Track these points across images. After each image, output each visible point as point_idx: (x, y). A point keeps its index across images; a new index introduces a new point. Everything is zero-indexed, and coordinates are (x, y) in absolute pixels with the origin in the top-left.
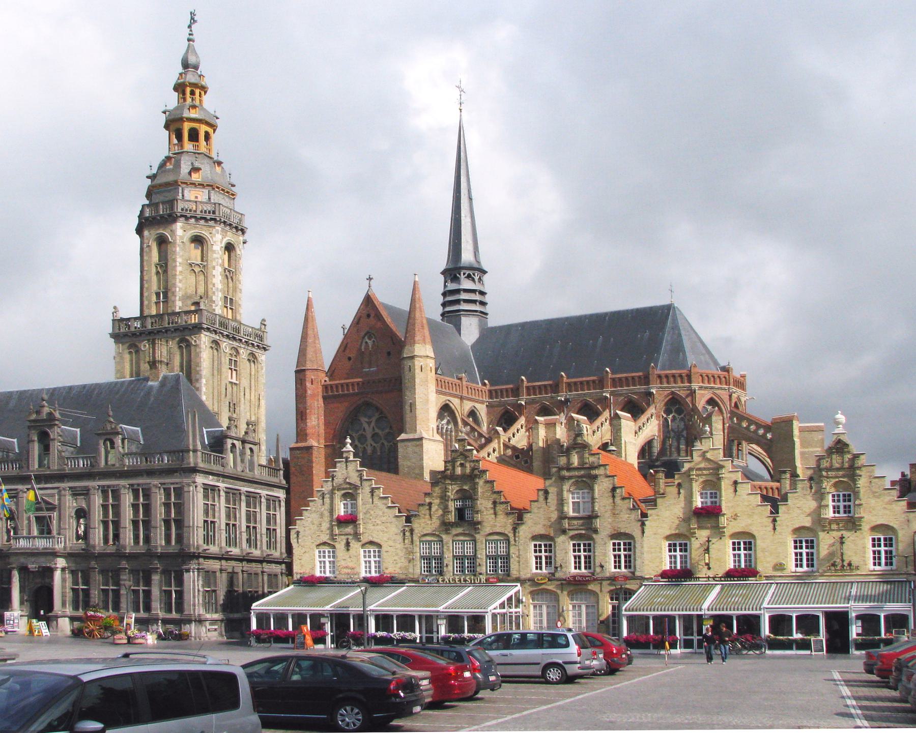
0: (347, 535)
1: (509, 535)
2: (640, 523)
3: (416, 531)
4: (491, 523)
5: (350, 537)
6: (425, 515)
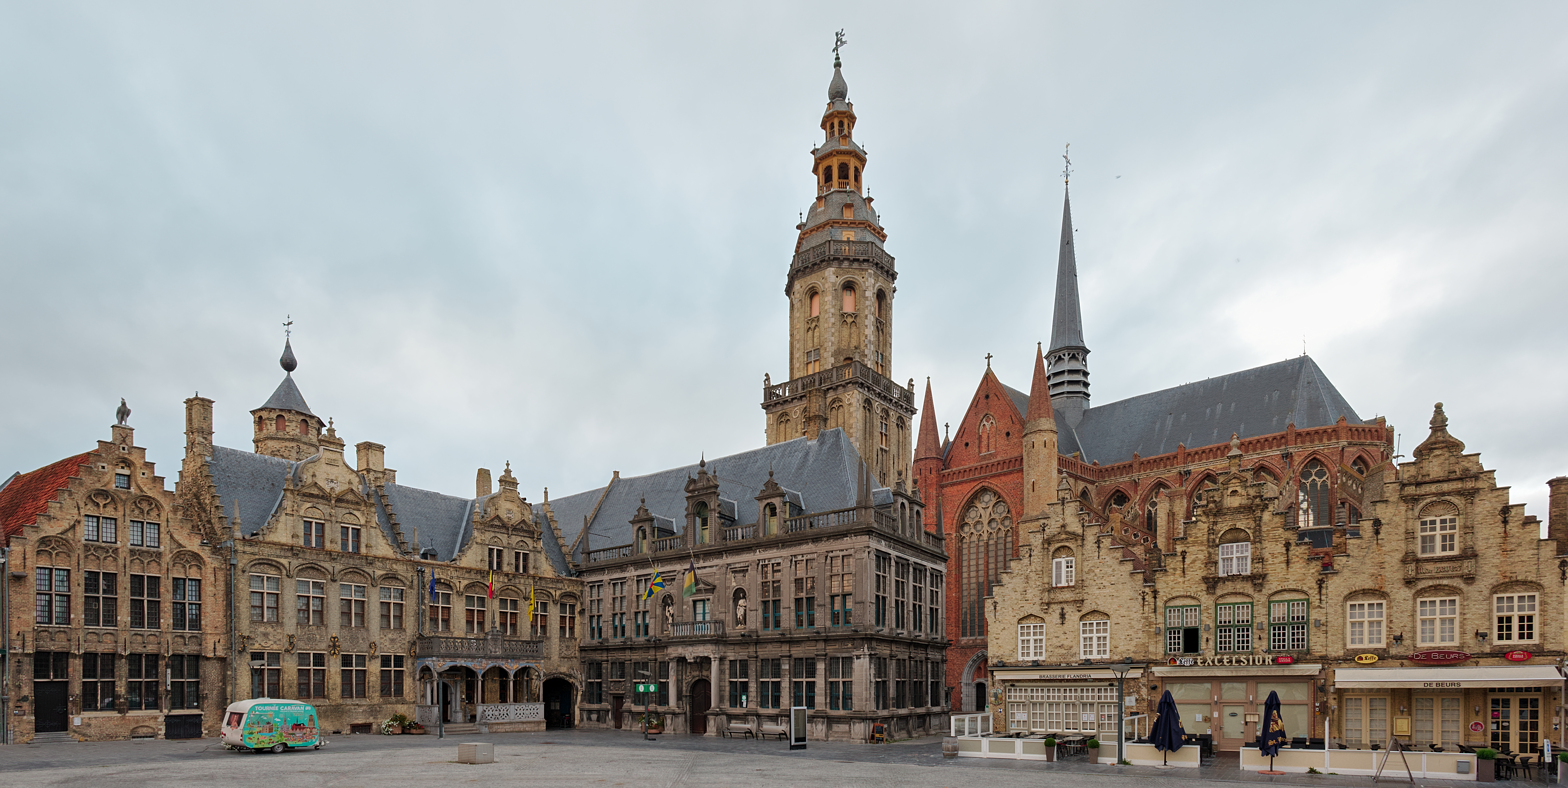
0: (1061, 603)
1: (1310, 592)
3: (1161, 594)
4: (1281, 575)
5: (1065, 606)
6: (1175, 569)
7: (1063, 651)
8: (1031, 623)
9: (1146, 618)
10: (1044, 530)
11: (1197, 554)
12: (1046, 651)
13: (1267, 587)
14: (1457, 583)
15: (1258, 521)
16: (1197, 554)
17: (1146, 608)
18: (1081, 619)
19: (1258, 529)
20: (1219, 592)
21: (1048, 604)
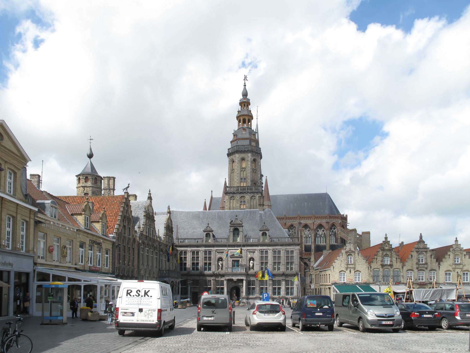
2: (438, 266)
5: (351, 269)
6: (375, 262)
7: (350, 280)
8: (342, 272)
9: (369, 273)
10: (345, 249)
11: (379, 259)
12: (346, 280)
13: (393, 267)
14: (424, 269)
15: (391, 252)
16: (379, 259)
17: (369, 271)
18: (355, 272)
19: (391, 255)
20: (384, 268)
21: (347, 268)
